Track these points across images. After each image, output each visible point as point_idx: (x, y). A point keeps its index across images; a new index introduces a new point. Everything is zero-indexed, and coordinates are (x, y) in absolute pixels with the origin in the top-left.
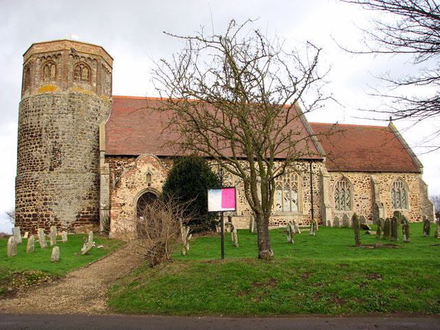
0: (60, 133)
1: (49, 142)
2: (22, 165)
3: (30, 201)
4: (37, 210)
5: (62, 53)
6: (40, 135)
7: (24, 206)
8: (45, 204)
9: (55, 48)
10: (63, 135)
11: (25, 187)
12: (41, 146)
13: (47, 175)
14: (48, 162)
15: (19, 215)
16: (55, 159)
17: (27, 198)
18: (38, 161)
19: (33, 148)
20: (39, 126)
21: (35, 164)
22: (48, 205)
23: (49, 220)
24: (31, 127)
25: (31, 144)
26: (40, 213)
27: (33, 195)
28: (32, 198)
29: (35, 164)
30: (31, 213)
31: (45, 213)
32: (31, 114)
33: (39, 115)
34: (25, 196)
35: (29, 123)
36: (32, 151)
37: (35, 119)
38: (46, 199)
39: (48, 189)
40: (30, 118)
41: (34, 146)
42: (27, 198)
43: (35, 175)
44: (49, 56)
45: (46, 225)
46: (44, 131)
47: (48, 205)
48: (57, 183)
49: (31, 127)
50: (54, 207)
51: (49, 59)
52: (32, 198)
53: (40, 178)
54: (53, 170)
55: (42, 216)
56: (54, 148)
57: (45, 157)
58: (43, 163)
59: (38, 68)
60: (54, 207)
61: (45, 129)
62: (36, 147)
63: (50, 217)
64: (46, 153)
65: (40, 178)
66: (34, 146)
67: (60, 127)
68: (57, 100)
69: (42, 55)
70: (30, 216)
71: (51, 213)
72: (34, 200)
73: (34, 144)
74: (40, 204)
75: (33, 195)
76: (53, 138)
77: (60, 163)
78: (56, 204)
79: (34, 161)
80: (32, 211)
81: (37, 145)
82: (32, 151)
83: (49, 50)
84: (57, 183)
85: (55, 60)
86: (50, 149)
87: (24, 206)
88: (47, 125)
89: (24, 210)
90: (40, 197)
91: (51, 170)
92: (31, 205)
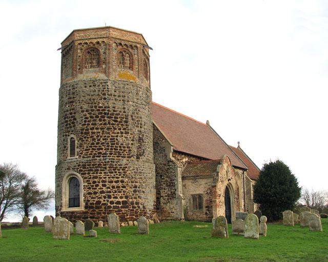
0: (143, 123)
1: (136, 130)
2: (102, 149)
3: (118, 187)
4: (127, 197)
5: (138, 46)
6: (126, 122)
7: (110, 192)
8: (135, 191)
9: (131, 38)
10: (145, 125)
11: (112, 173)
12: (127, 133)
13: (136, 163)
14: (134, 150)
15: (99, 202)
16: (140, 148)
17: (114, 184)
18: (124, 147)
19: (118, 133)
20: (124, 112)
21: (121, 150)
22: (137, 193)
23: (139, 207)
24: (114, 111)
25: (115, 129)
26: (131, 200)
27: (122, 181)
28: (120, 184)
29: (121, 150)
30: (121, 200)
31: (135, 200)
32: (112, 97)
33: (123, 100)
34: (111, 182)
35: (111, 105)
36: (117, 136)
37: (119, 105)
38: (136, 187)
39: (137, 177)
40: (111, 101)
41: (119, 131)
42: (114, 184)
43: (125, 161)
44: (125, 45)
45: (136, 212)
46: (130, 118)
47: (137, 193)
48: (144, 171)
49: (114, 111)
50: (143, 196)
51: (124, 47)
52: (120, 184)
53: (129, 165)
54: (139, 159)
55: (132, 203)
56: (139, 137)
57: (132, 144)
58: (130, 150)
59: (115, 53)
60: (143, 196)
61: (132, 116)
62: (122, 133)
63: (140, 205)
64: (133, 140)
65: (129, 165)
66: (119, 131)
67: (143, 117)
68: (140, 91)
69: (118, 41)
70: (118, 203)
71: (140, 201)
72: (124, 187)
73: (120, 129)
74: (129, 191)
75: (122, 181)
76: (138, 127)
77: (144, 152)
78: (143, 192)
79: (120, 147)
80: (121, 198)
81: (122, 130)
82: (117, 136)
83: (125, 38)
84: (144, 171)
85: (130, 50)
86: (136, 137)
87: (110, 192)
88: (133, 113)
89: (110, 197)
90: (130, 184)
91: (138, 158)
92: (120, 192)
